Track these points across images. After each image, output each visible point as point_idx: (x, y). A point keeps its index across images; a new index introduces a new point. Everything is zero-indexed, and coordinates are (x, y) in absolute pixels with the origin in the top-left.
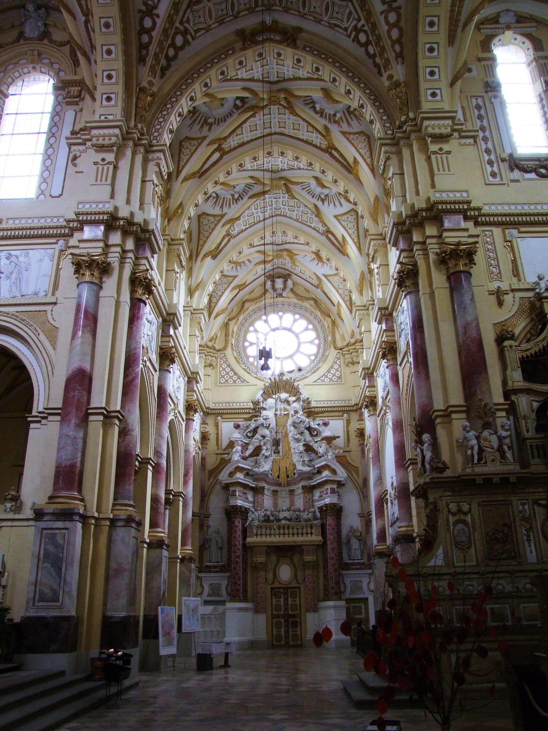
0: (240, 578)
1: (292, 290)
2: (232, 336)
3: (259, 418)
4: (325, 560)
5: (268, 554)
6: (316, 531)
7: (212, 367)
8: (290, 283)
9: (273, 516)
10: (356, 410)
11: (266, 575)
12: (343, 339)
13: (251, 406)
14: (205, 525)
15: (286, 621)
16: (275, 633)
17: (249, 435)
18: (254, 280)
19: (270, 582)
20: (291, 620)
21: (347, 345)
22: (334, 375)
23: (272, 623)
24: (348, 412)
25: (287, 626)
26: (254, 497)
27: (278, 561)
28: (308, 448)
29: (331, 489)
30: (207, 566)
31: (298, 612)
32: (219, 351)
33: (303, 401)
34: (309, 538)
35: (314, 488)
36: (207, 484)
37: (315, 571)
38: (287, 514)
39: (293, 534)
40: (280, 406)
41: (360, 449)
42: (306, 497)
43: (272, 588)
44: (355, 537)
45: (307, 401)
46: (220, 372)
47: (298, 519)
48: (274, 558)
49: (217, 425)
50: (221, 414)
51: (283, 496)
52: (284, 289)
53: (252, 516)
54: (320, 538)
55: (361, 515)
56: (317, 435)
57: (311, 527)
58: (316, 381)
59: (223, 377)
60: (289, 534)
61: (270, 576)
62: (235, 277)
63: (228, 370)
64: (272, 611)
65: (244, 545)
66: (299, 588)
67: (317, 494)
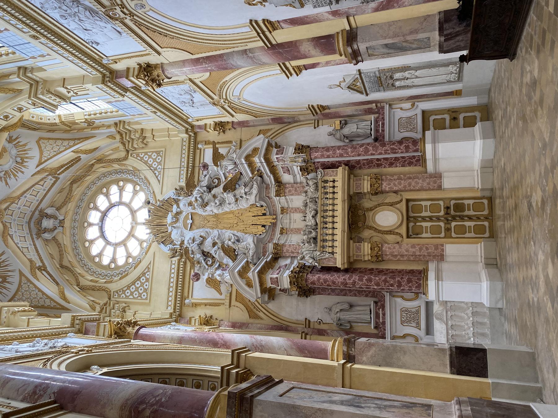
1: (58, 209)
2: (97, 282)
3: (190, 249)
4: (370, 163)
5: (360, 240)
6: (330, 175)
7: (127, 309)
8: (49, 211)
9: (311, 232)
10: (195, 134)
11: (388, 244)
12: (116, 150)
13: (176, 259)
14: (317, 326)
15: (454, 218)
16: (472, 235)
17: (209, 263)
18: (37, 251)
21: (124, 145)
22: (155, 160)
24: (196, 143)
25: (462, 218)
26: (286, 257)
27: (370, 228)
28: (230, 187)
29: (277, 154)
32: (110, 299)
33: (179, 195)
34: (339, 184)
35: (278, 181)
36: (267, 321)
37: (384, 177)
38: (309, 216)
40: (180, 224)
41: (239, 129)
43: (408, 237)
44: (342, 128)
45: (179, 191)
46: (134, 298)
47: (314, 201)
48: (367, 233)
49: (195, 305)
50: (183, 298)
51: (288, 221)
52: (55, 218)
53: (307, 258)
54: (340, 169)
55: (317, 125)
56: (219, 179)
57: (326, 182)
59: (140, 295)
60: (333, 210)
61: (390, 238)
62: (21, 274)
63: (133, 289)
64: (440, 238)
65: (346, 271)
66: (408, 201)
67: (286, 178)
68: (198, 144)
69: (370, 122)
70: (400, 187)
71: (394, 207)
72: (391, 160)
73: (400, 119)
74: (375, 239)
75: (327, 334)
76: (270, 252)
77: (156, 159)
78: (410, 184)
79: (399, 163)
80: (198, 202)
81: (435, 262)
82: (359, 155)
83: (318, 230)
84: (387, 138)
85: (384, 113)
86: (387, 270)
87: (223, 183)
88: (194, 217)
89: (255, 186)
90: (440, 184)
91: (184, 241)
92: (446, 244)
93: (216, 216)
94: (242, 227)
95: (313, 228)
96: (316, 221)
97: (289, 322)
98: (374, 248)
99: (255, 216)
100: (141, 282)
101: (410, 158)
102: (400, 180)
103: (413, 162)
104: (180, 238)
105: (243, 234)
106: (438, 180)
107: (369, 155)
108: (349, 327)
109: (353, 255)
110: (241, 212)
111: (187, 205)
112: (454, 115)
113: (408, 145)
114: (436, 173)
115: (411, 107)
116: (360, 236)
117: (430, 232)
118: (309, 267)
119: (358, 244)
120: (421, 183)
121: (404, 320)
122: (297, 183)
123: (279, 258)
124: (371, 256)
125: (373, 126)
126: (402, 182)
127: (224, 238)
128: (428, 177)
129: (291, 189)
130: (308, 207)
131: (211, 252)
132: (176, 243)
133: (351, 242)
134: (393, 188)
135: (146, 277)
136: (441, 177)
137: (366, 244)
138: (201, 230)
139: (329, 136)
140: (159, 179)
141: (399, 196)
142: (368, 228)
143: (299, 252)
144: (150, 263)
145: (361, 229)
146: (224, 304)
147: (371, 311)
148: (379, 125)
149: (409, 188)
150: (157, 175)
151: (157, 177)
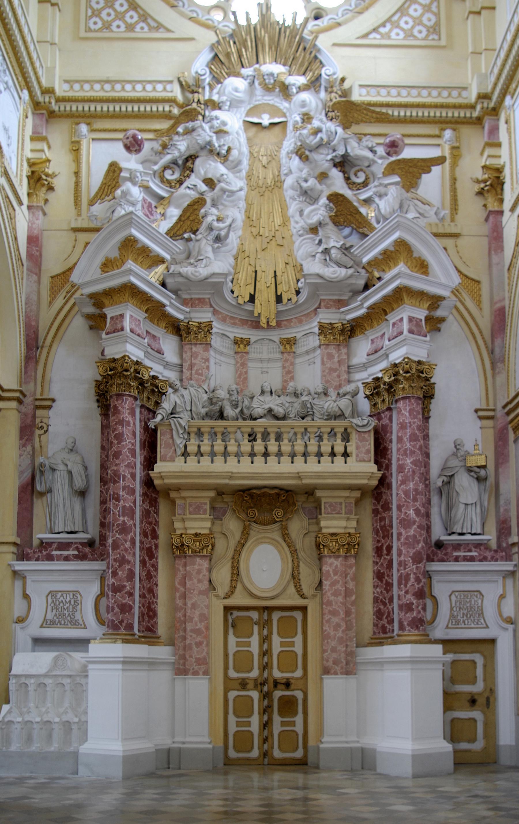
0: (131, 575)
9: (236, 406)
10: (479, 121)
11: (210, 570)
17: (168, 175)
19: (223, 588)
20: (278, 694)
22: (418, 21)
23: (226, 700)
27: (245, 535)
30: (41, 539)
31: (299, 673)
37: (352, 561)
39: (293, 455)
42: (330, 356)
43: (228, 609)
44: (469, 470)
56: (365, 184)
58: (365, 36)
66: (304, 609)
68: (454, 130)
69: (479, 531)
70: (329, 594)
71: (288, 583)
72: (388, 576)
73: (481, 594)
74: (220, 544)
75: (24, 445)
76: (193, 315)
77: (421, 23)
78: (334, 613)
79: (381, 592)
80: (312, 137)
81: (172, 659)
82: (399, 508)
83: (241, 422)
84: (435, 566)
85: (496, 560)
86: (155, 567)
87: (355, 195)
88: (277, 130)
89: (342, 272)
90: (332, 671)
91: (220, 108)
92: (210, 679)
93: (277, 184)
94: (251, 246)
95: (245, 411)
96: (261, 417)
97: (45, 364)
98: (200, 541)
99: (275, 276)
100: (126, 11)
101: (389, 613)
102: (343, 594)
103: (381, 619)
104: (224, 98)
105: (234, 252)
106: (342, 668)
107: (398, 529)
108: (39, 488)
109: (184, 498)
110: (285, 242)
111: (304, 110)
112: (481, 701)
113: (412, 610)
114: (355, 664)
115: (505, 615)
116: (229, 514)
117: (238, 651)
118: (157, 404)
119: (208, 507)
120: (335, 635)
121: (59, 596)
122: (349, 373)
123: (181, 336)
124: (181, 534)
125: (468, 537)
126: (340, 599)
127: (225, 206)
128: (349, 649)
129: (336, 360)
130: (294, 399)
131: (193, 176)
132: (215, 91)
133: (212, 494)
134: (327, 580)
135: (137, 23)
136: (348, 673)
137: (208, 524)
138: (245, 149)
139: (454, 443)
140: (372, 36)
141: (313, 591)
142: (245, 529)
143: (192, 382)
144: (168, 30)
145: (243, 516)
146: (79, 215)
147: (72, 532)
148: (470, 551)
149: (326, 611)
150: (382, 30)
151: (375, 30)
